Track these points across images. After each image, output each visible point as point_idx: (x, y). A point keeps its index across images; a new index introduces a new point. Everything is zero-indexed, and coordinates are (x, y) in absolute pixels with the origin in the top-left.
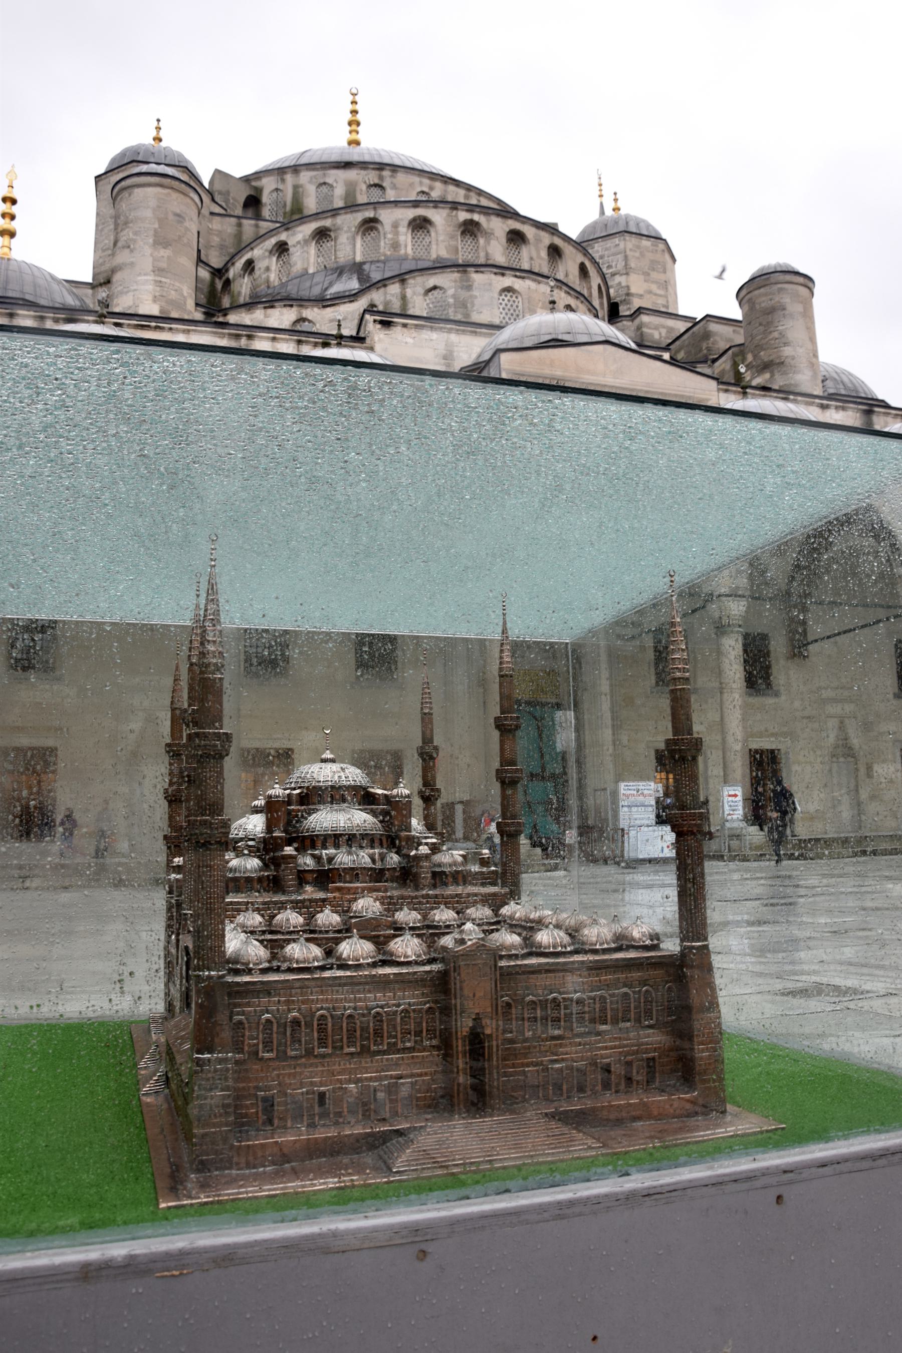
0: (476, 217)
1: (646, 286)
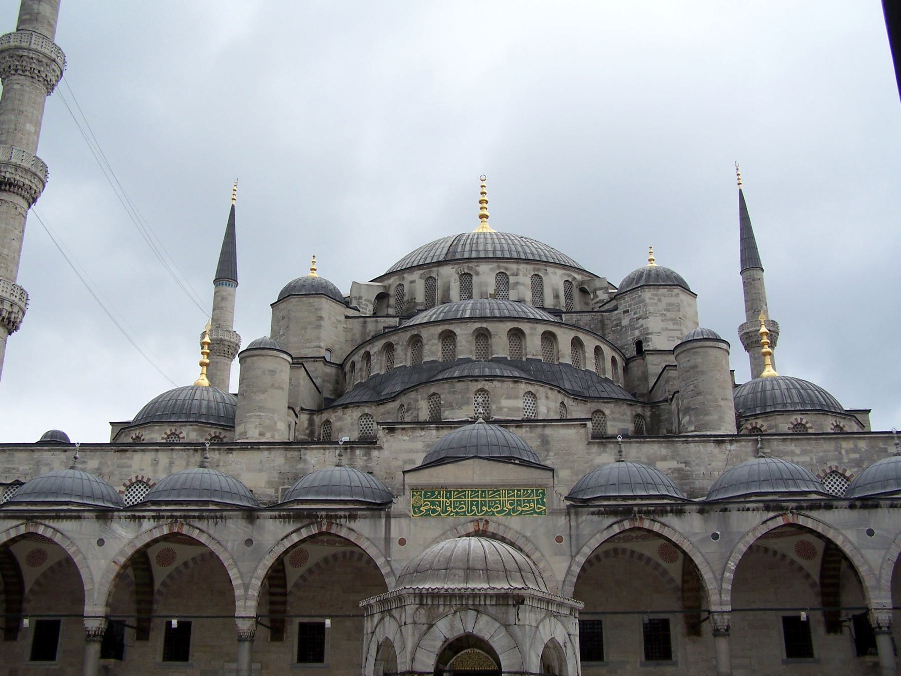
0: (484, 325)
1: (662, 325)
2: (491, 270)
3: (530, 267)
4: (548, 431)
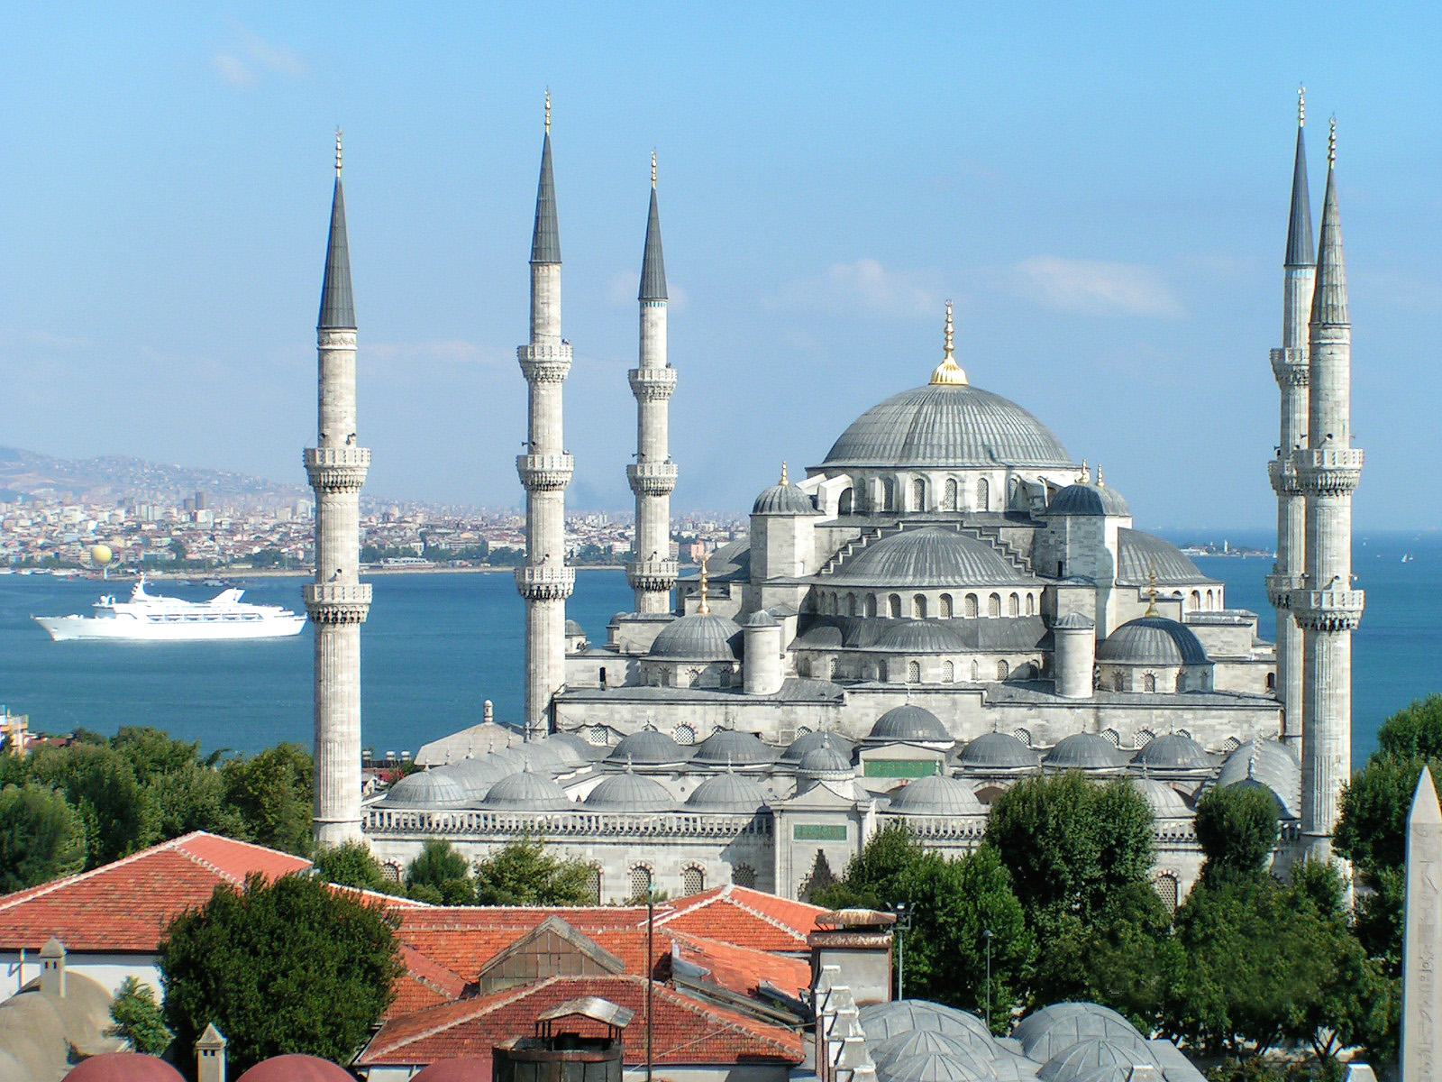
0: (922, 592)
1: (1081, 551)
2: (942, 477)
3: (976, 473)
4: (956, 696)
